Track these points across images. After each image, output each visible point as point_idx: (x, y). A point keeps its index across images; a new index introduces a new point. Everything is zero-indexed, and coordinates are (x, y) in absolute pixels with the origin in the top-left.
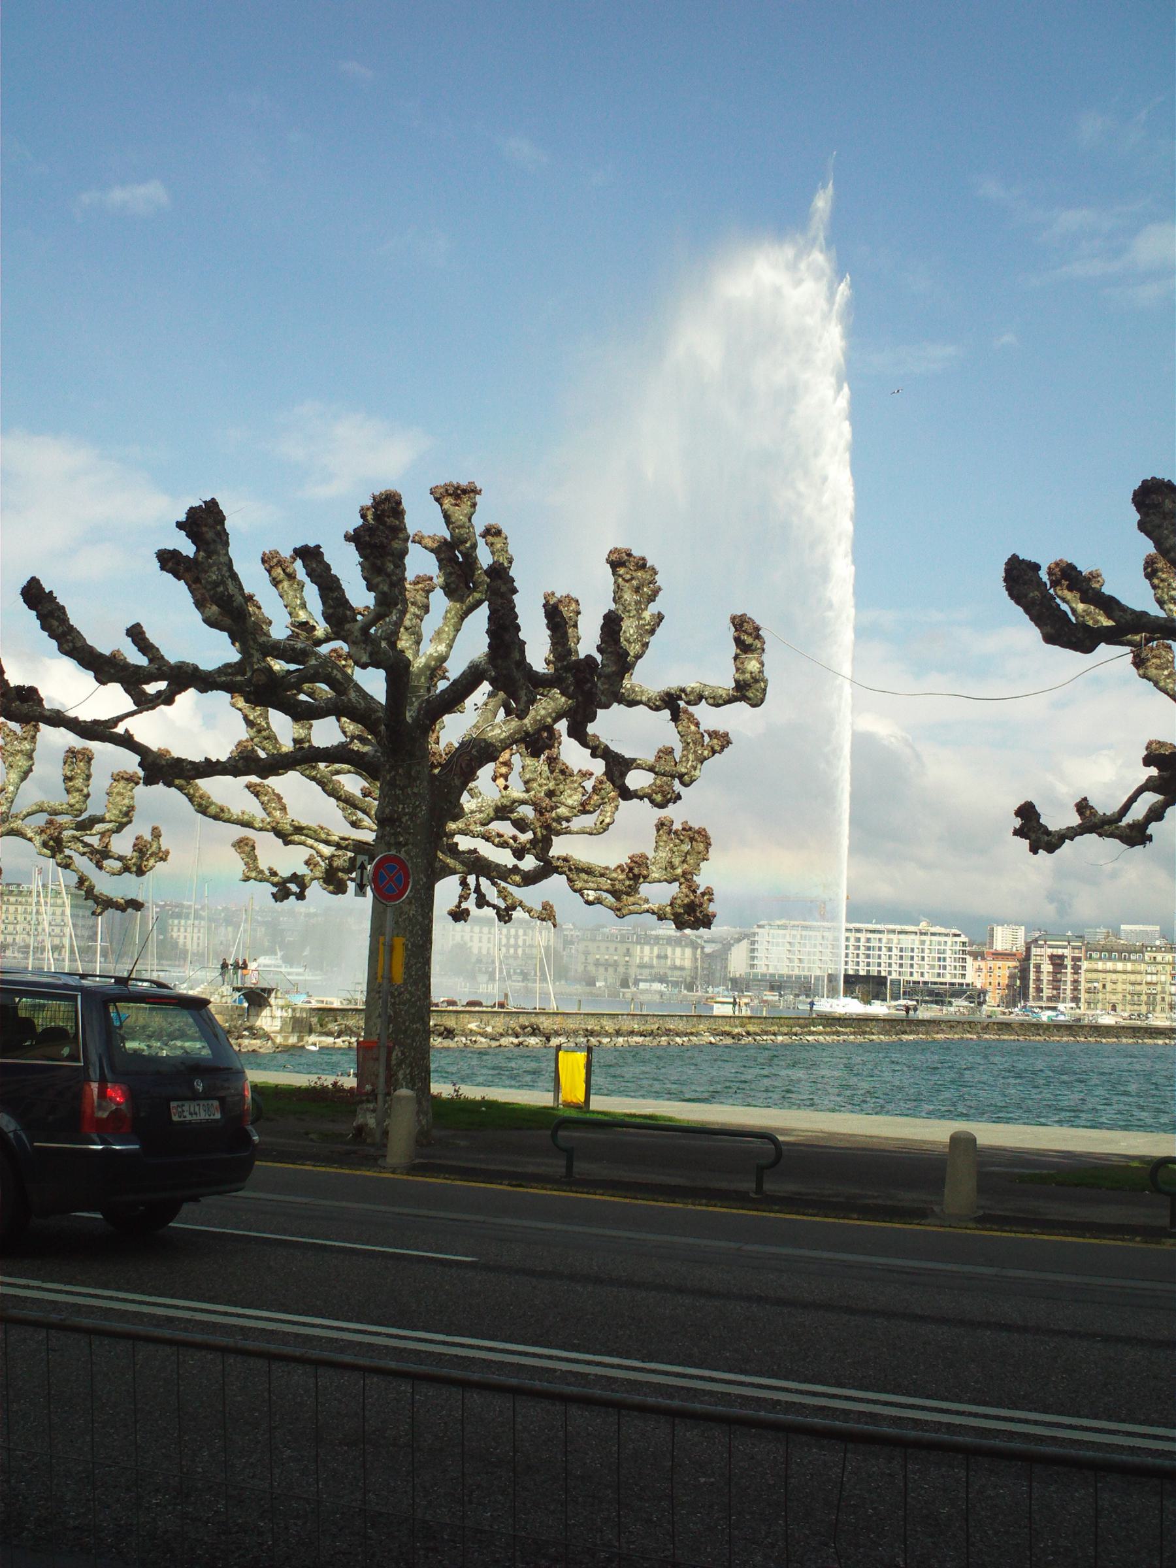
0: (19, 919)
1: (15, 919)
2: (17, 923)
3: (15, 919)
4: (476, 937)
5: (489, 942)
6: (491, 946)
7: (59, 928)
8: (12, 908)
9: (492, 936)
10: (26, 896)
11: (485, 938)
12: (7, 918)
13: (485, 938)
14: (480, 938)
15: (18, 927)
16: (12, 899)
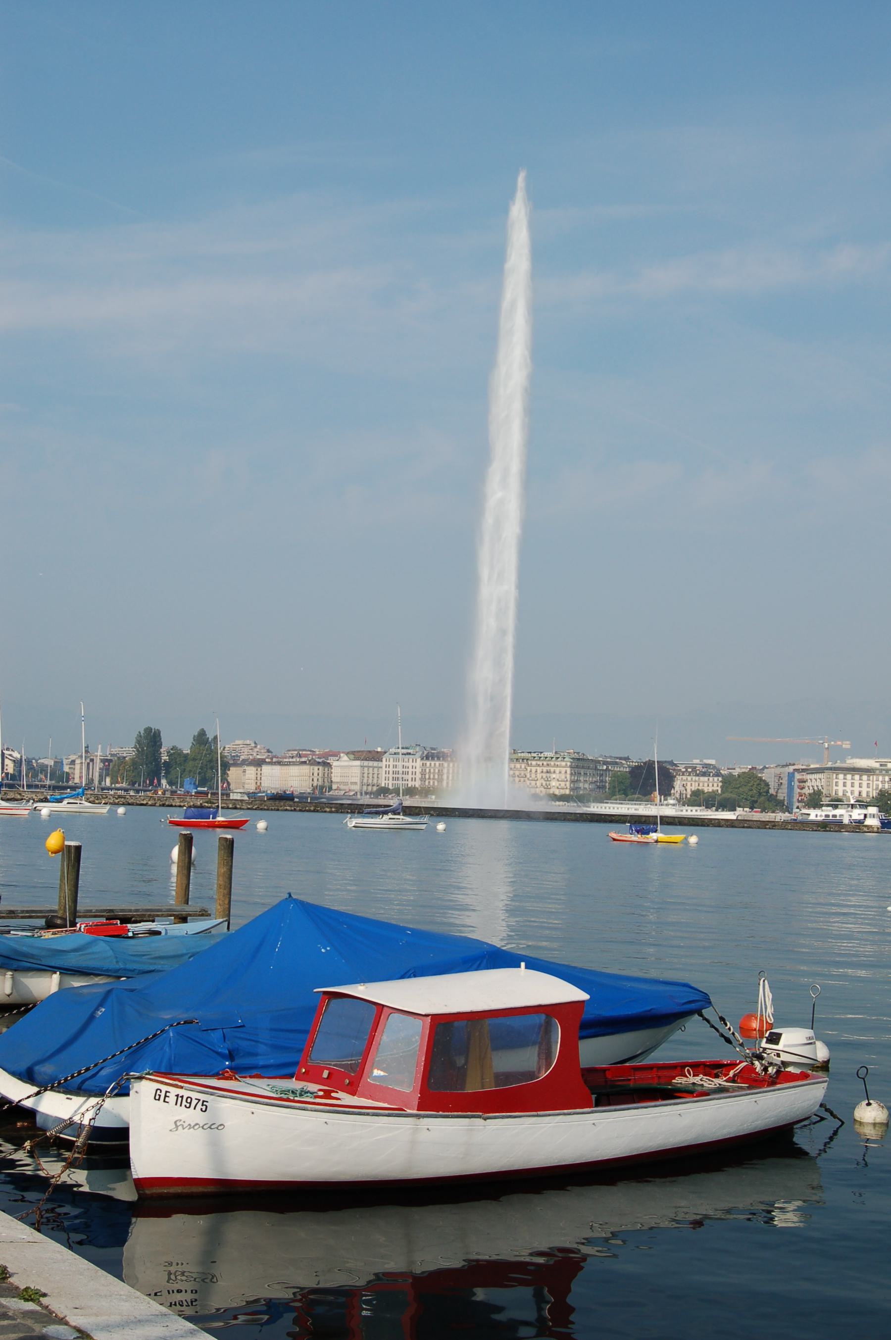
0: (538, 777)
1: (536, 777)
2: (537, 780)
3: (536, 777)
4: (841, 783)
5: (868, 787)
6: (870, 790)
7: (534, 782)
8: (534, 769)
9: (871, 782)
10: (549, 761)
11: (865, 784)
12: (531, 777)
13: (865, 784)
14: (844, 783)
15: (538, 782)
16: (534, 763)
